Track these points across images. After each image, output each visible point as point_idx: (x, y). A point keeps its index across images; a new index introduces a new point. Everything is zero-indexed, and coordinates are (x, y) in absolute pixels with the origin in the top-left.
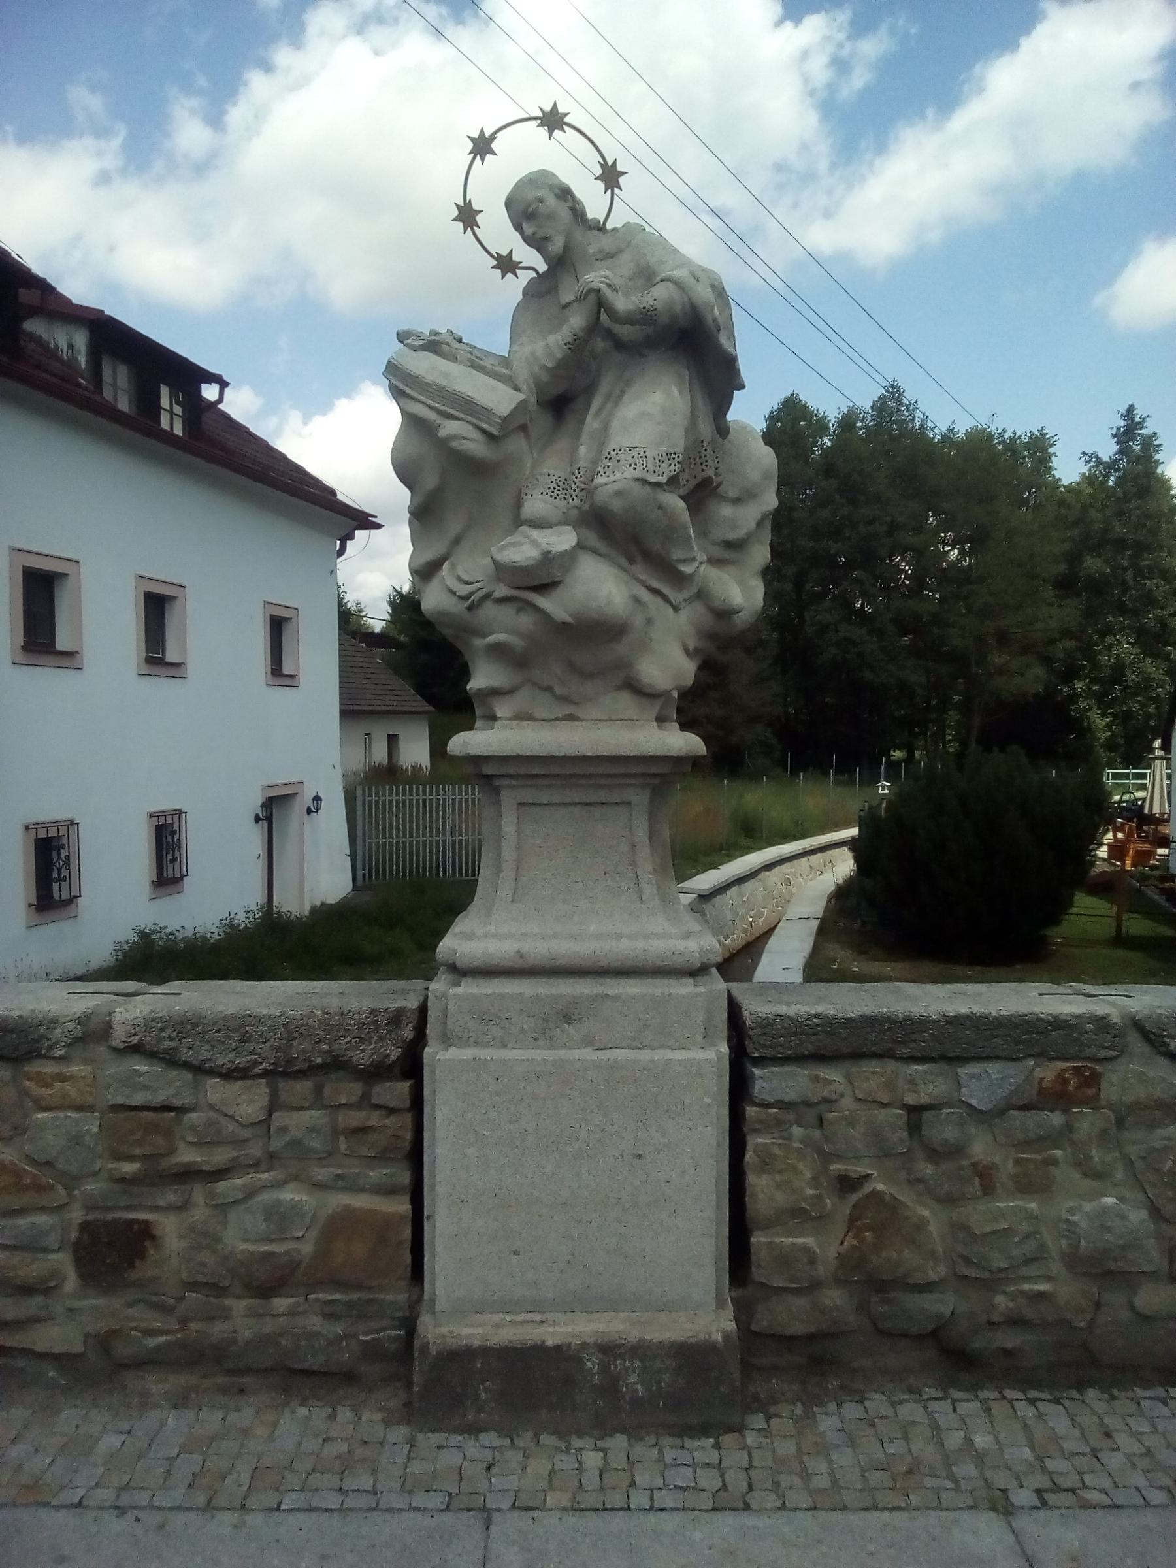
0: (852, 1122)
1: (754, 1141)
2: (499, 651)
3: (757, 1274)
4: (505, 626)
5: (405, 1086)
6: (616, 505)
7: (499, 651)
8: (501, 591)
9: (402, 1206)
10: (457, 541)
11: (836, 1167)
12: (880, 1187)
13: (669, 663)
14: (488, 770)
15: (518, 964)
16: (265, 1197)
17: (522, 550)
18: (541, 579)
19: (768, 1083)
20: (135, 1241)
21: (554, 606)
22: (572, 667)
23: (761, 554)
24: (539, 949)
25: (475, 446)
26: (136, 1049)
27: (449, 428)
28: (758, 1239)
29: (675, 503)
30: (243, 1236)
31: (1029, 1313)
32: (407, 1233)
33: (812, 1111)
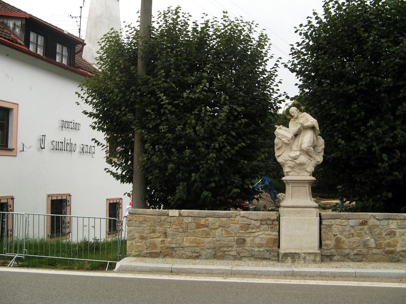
0: (335, 227)
1: (323, 230)
2: (289, 167)
3: (323, 247)
4: (291, 164)
5: (278, 222)
6: (305, 149)
7: (289, 167)
8: (290, 159)
9: (277, 237)
10: (283, 153)
11: (334, 233)
12: (339, 236)
13: (311, 169)
14: (288, 182)
15: (292, 206)
16: (260, 236)
17: (293, 154)
18: (295, 158)
19: (324, 222)
20: (244, 241)
21: (297, 161)
22: (299, 169)
23: (323, 154)
24: (295, 205)
25: (287, 142)
26: (243, 217)
27: (283, 139)
28: (323, 242)
29: (312, 148)
30: (257, 240)
31: (359, 253)
32: (278, 241)
33: (330, 226)
